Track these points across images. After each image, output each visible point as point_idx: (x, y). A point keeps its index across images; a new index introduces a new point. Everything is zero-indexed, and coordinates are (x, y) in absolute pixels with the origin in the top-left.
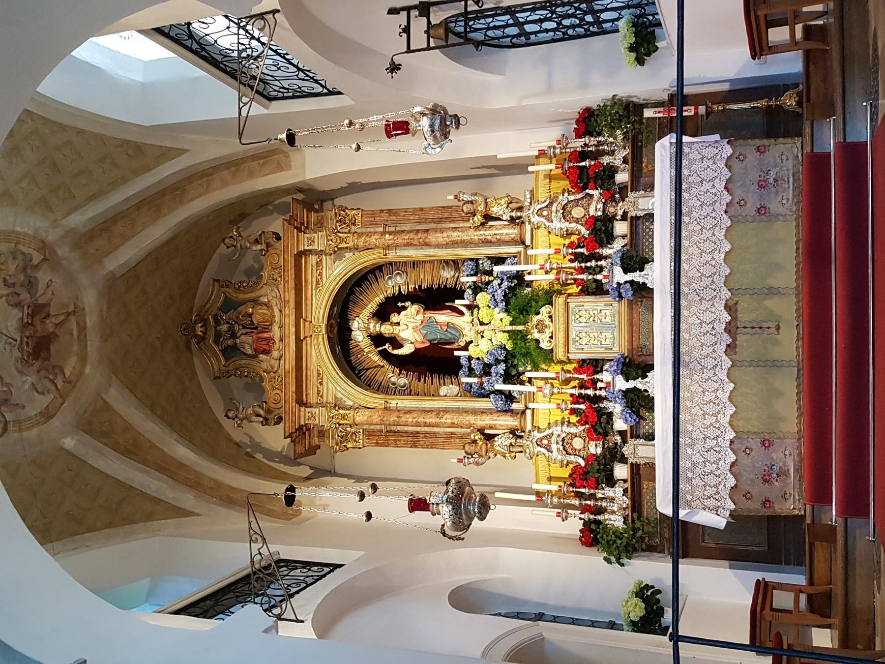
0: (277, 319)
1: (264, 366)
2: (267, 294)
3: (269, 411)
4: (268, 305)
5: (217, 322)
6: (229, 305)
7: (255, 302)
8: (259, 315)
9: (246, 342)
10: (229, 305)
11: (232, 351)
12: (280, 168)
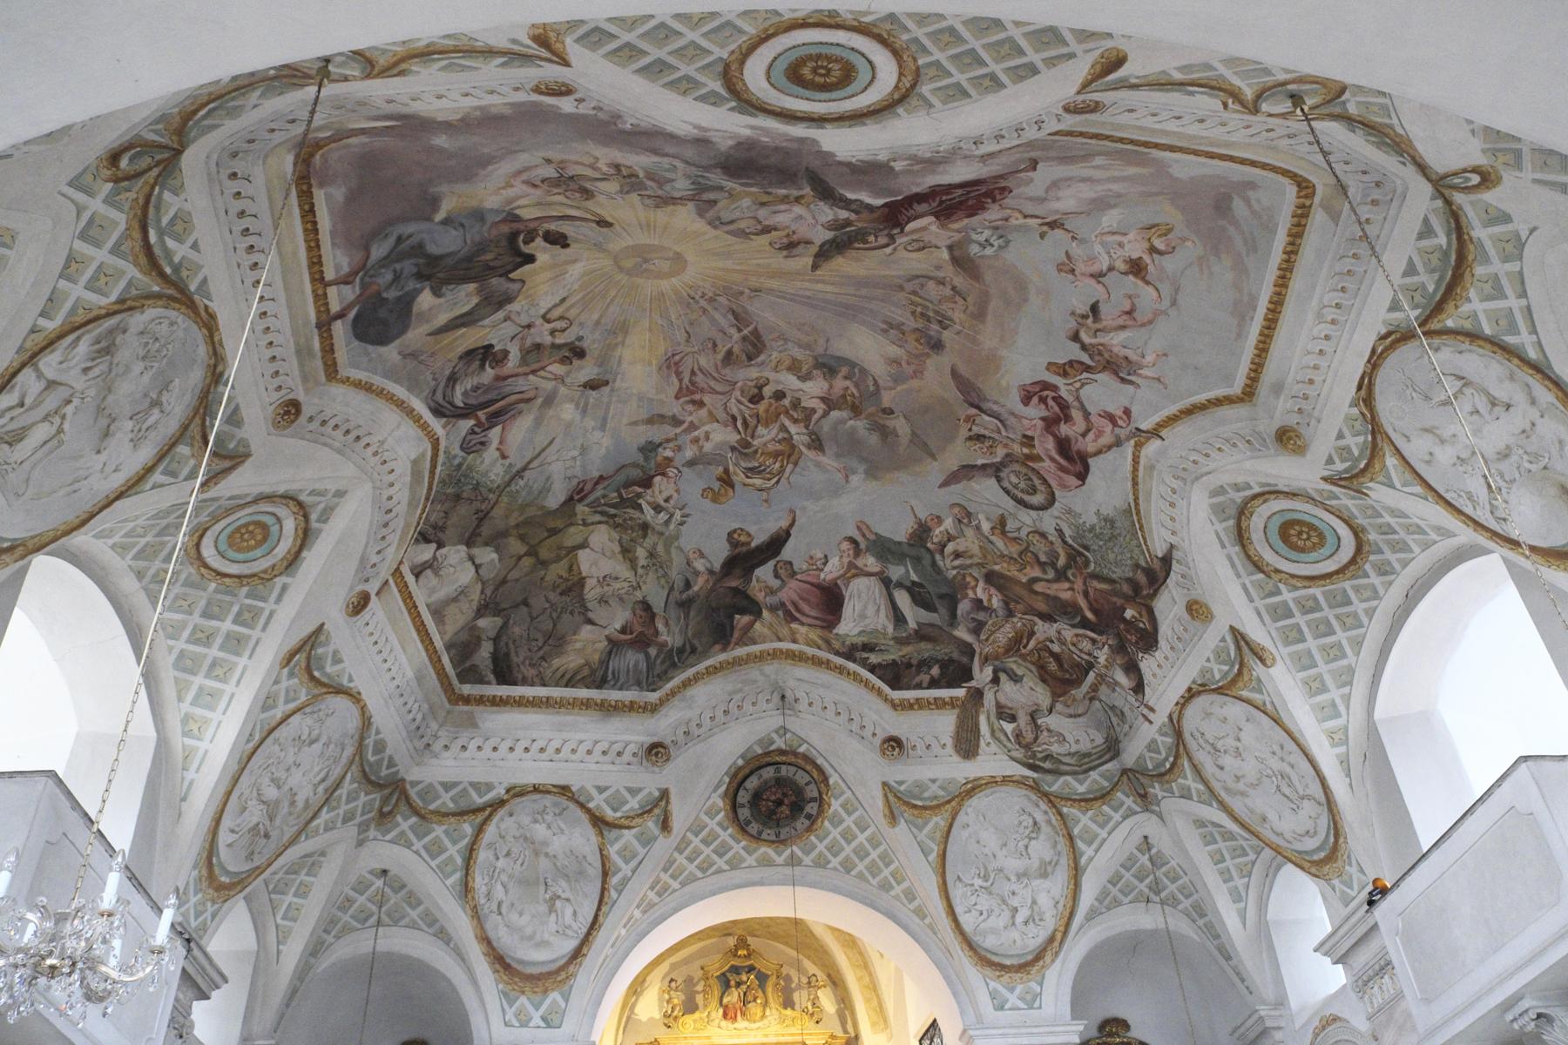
0: (754, 1026)
1: (714, 1014)
2: (773, 1012)
3: (676, 1018)
4: (763, 1016)
5: (751, 969)
6: (762, 978)
7: (765, 1004)
8: (755, 1009)
9: (733, 997)
10: (762, 978)
11: (726, 985)
12: (874, 1024)
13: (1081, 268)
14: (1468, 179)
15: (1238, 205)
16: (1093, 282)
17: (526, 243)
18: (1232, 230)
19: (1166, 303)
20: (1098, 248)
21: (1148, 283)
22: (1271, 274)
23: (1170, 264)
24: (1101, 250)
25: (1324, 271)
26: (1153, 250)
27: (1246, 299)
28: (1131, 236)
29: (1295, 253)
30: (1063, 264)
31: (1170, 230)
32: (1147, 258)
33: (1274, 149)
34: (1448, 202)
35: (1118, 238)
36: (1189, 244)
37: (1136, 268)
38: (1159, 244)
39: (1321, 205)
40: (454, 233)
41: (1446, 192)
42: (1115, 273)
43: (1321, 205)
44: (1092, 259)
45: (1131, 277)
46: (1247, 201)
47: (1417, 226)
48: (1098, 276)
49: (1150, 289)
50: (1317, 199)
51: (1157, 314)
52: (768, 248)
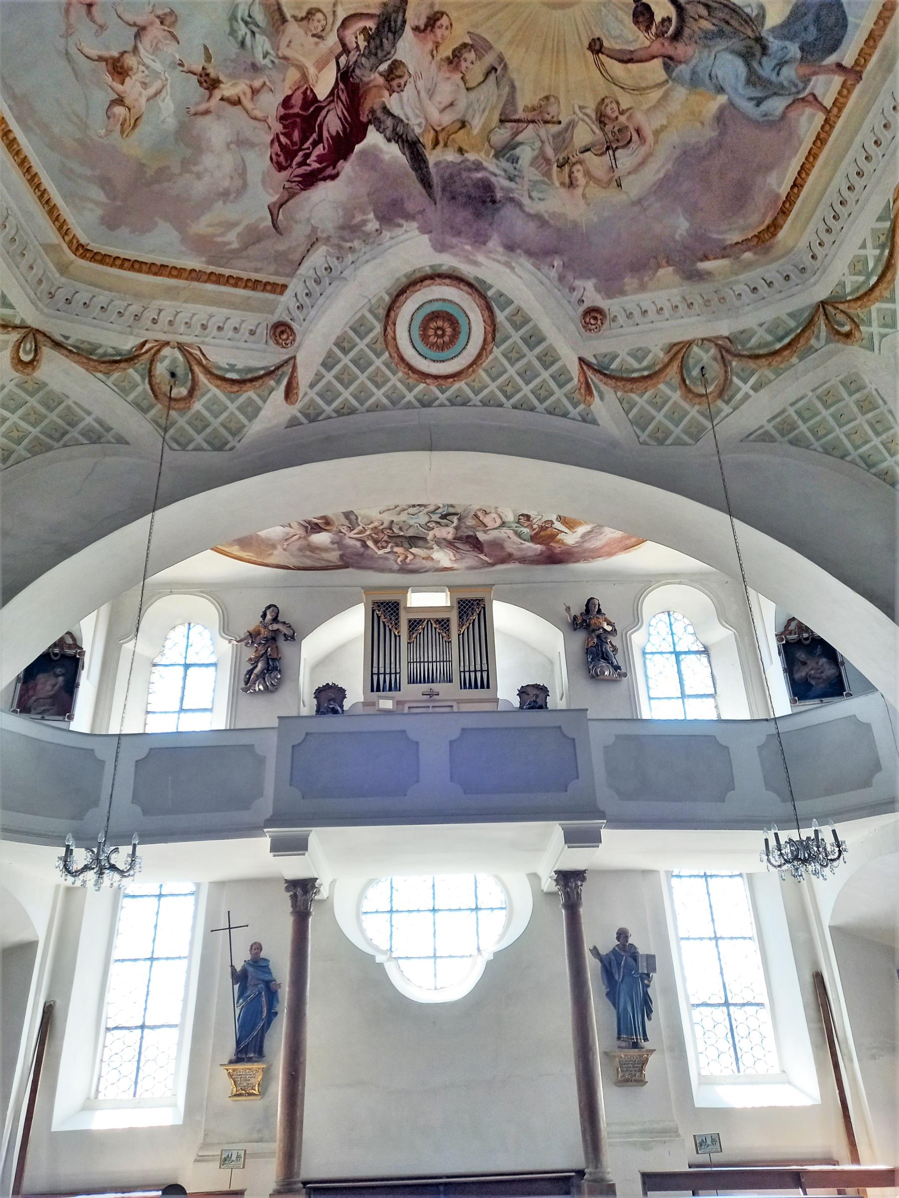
13: (156, 31)
14: (27, 353)
15: (101, 197)
16: (141, 20)
17: (669, 19)
18: (89, 173)
19: (73, 51)
20: (158, 66)
21: (101, 59)
22: (37, 166)
23: (102, 98)
24: (152, 64)
25: (15, 207)
26: (120, 101)
27: (30, 122)
28: (143, 100)
29: (41, 197)
30: (174, 23)
31: (122, 132)
32: (118, 87)
33: (137, 296)
34: (15, 327)
35: (151, 91)
36: (102, 132)
37: (118, 69)
38: (119, 110)
39: (59, 245)
40: (720, 75)
41: (25, 330)
42: (129, 48)
43: (59, 245)
44: (156, 49)
45: (116, 54)
46: (97, 203)
47: (11, 299)
48: (140, 31)
49: (94, 53)
50: (65, 247)
51: (69, 32)
52: (453, 15)
